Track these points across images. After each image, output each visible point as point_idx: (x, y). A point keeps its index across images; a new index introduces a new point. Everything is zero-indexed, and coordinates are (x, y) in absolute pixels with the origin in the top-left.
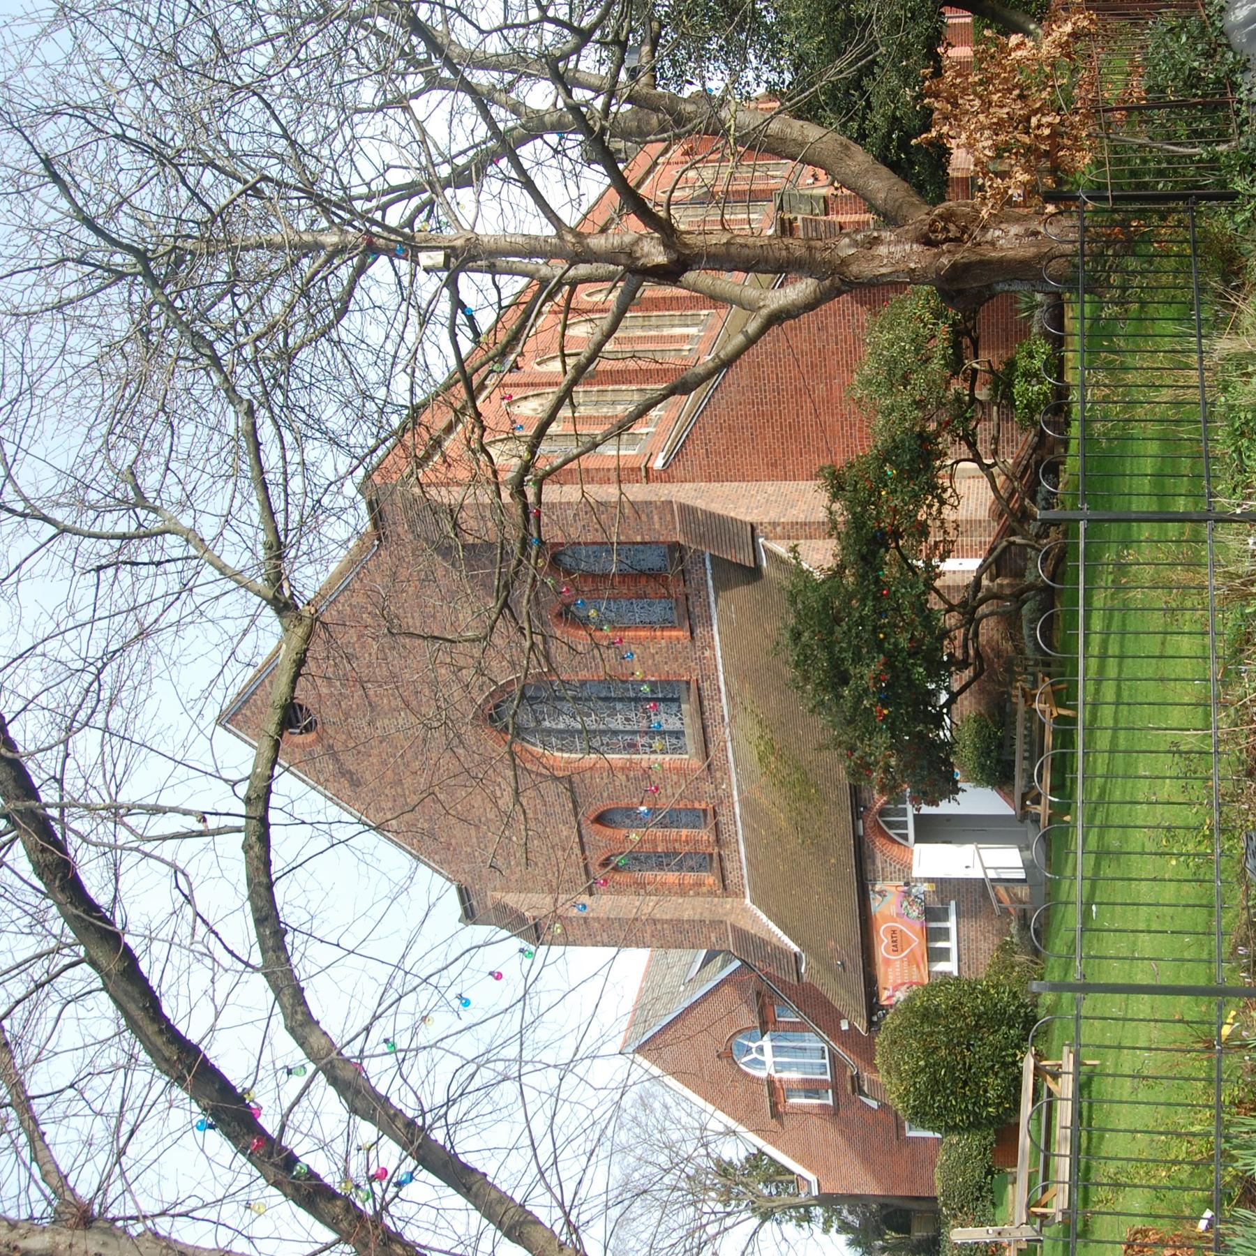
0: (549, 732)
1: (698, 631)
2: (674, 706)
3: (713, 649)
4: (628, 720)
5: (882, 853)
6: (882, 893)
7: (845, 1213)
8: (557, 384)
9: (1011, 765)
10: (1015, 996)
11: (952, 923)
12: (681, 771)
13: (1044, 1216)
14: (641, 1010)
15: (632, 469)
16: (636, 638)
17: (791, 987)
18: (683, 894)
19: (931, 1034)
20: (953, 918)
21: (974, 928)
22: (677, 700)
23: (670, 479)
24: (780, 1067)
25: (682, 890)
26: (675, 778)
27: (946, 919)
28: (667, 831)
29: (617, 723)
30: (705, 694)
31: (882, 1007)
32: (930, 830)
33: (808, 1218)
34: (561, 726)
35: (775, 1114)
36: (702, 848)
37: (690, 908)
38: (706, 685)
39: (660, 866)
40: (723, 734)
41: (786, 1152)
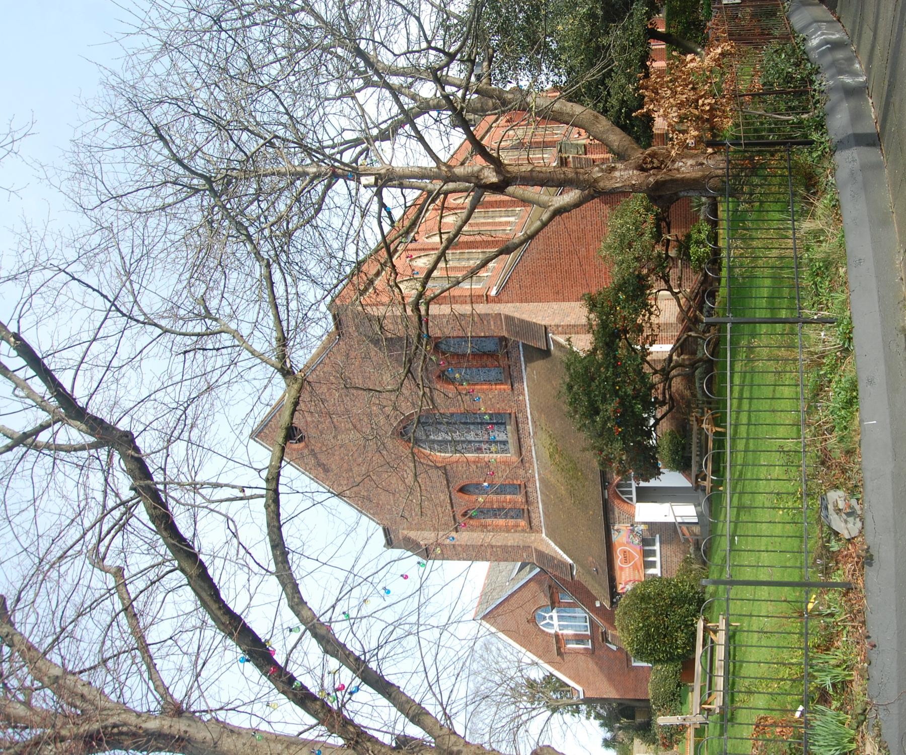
0: (434, 442)
1: (516, 385)
2: (502, 427)
3: (524, 395)
4: (477, 435)
5: (618, 508)
6: (618, 531)
7: (598, 708)
8: (437, 249)
9: (690, 459)
10: (692, 587)
11: (657, 547)
12: (506, 463)
13: (709, 710)
14: (485, 596)
15: (479, 296)
16: (483, 391)
17: (568, 582)
18: (508, 531)
19: (646, 609)
20: (658, 544)
21: (669, 550)
22: (504, 424)
23: (500, 301)
24: (562, 627)
25: (508, 530)
26: (503, 467)
27: (654, 545)
28: (499, 497)
29: (471, 437)
30: (520, 420)
31: (619, 594)
32: (645, 495)
33: (578, 711)
34: (440, 438)
35: (560, 653)
36: (518, 506)
37: (512, 539)
38: (520, 415)
39: (495, 516)
40: (530, 442)
41: (565, 674)
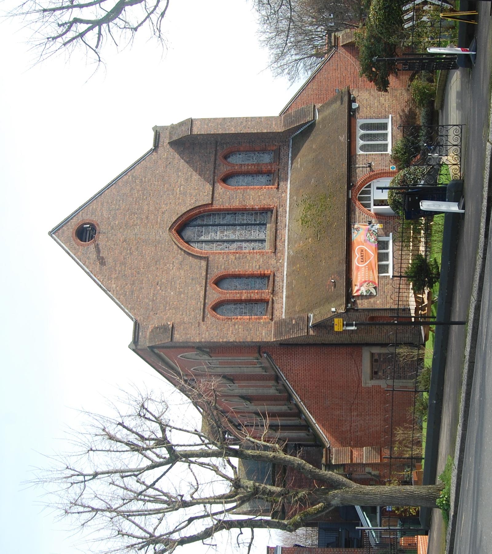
1: (281, 184)
2: (263, 227)
3: (286, 192)
22: (265, 224)
30: (279, 214)
31: (354, 297)
40: (285, 234)
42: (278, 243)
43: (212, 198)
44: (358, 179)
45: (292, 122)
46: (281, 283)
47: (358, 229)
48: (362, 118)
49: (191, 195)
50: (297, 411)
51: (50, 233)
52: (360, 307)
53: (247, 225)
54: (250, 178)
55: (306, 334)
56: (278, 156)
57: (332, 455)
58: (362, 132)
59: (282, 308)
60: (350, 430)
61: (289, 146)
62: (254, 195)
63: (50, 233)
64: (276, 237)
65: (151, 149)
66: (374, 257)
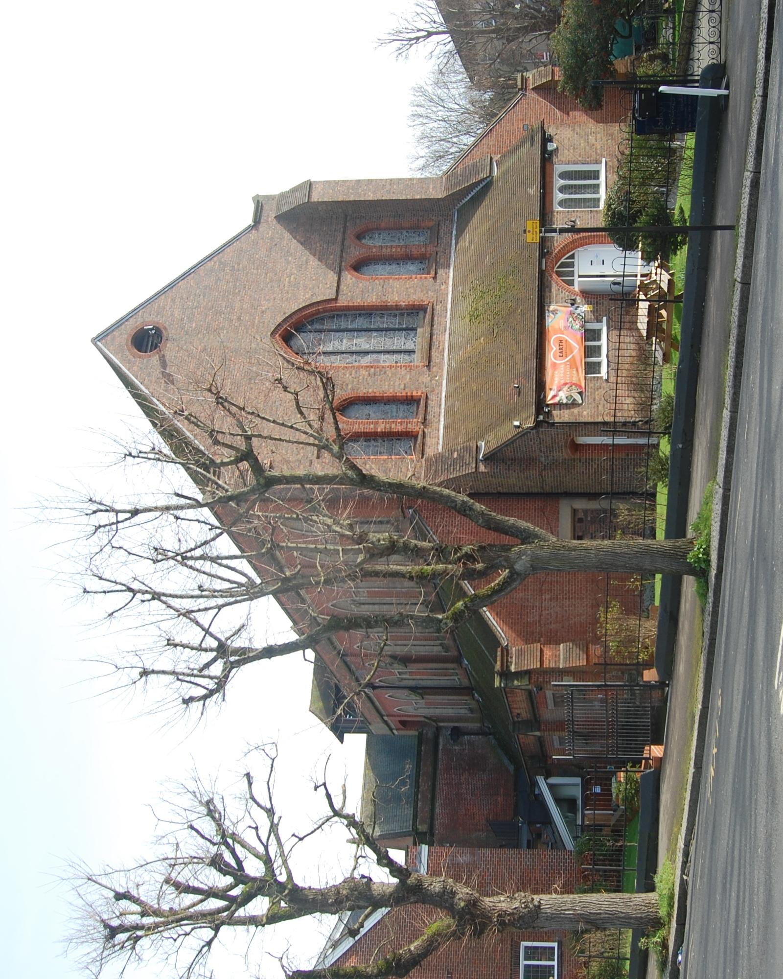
1: (441, 272)
2: (412, 334)
3: (446, 283)
8: (329, 639)
22: (415, 329)
30: (436, 313)
31: (548, 405)
40: (444, 340)
42: (434, 354)
43: (337, 291)
44: (556, 245)
45: (458, 184)
46: (437, 409)
47: (555, 312)
48: (562, 163)
49: (305, 287)
50: (456, 653)
51: (94, 341)
52: (557, 420)
53: (387, 330)
54: (394, 266)
55: (474, 470)
56: (435, 234)
57: (511, 658)
58: (562, 182)
59: (438, 443)
60: (539, 621)
61: (452, 221)
62: (398, 287)
63: (94, 341)
64: (430, 344)
65: (249, 226)
66: (580, 350)
